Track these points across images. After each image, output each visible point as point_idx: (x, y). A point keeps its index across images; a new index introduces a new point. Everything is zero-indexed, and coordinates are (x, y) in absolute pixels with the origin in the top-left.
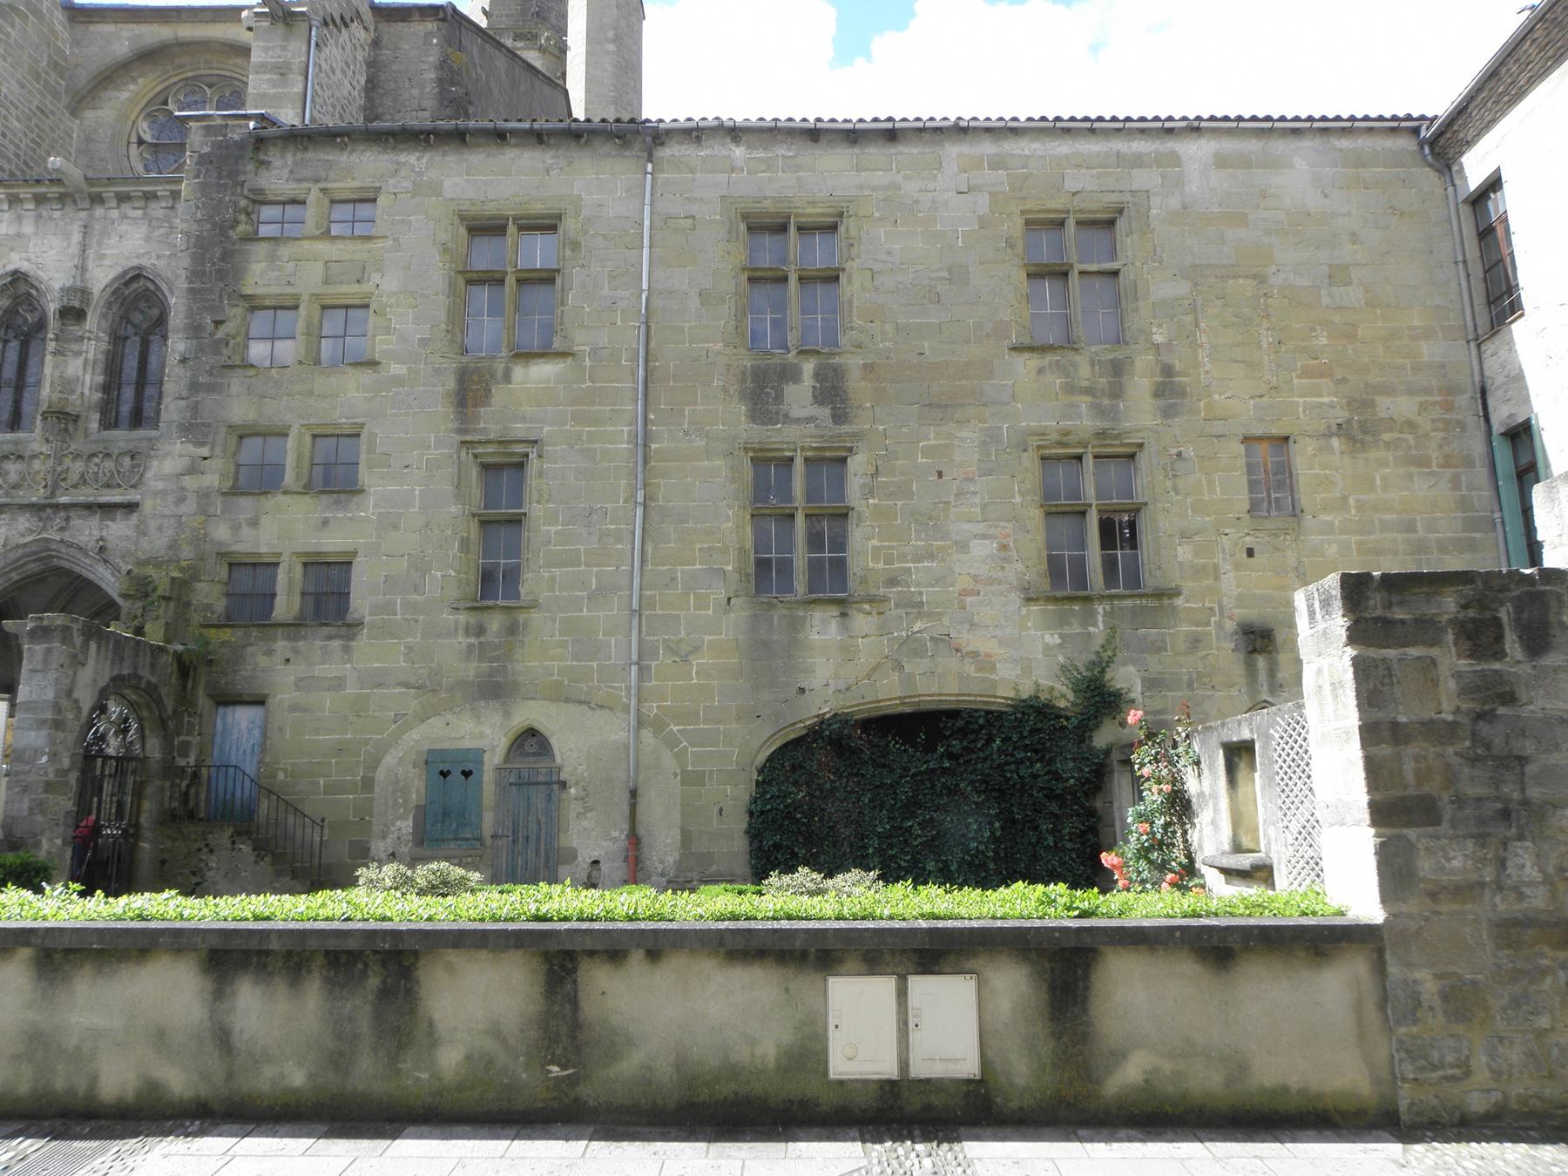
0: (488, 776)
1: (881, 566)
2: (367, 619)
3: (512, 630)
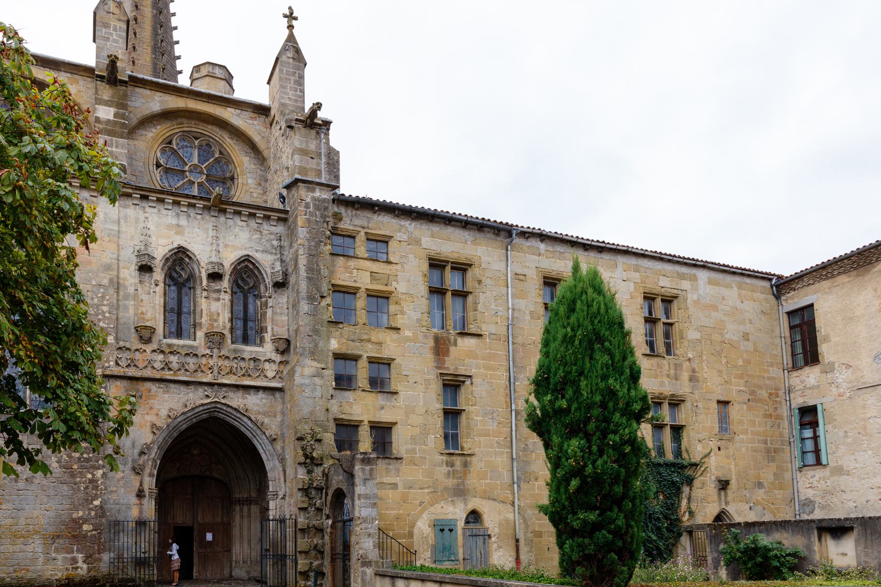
0: (460, 532)
3: (466, 465)
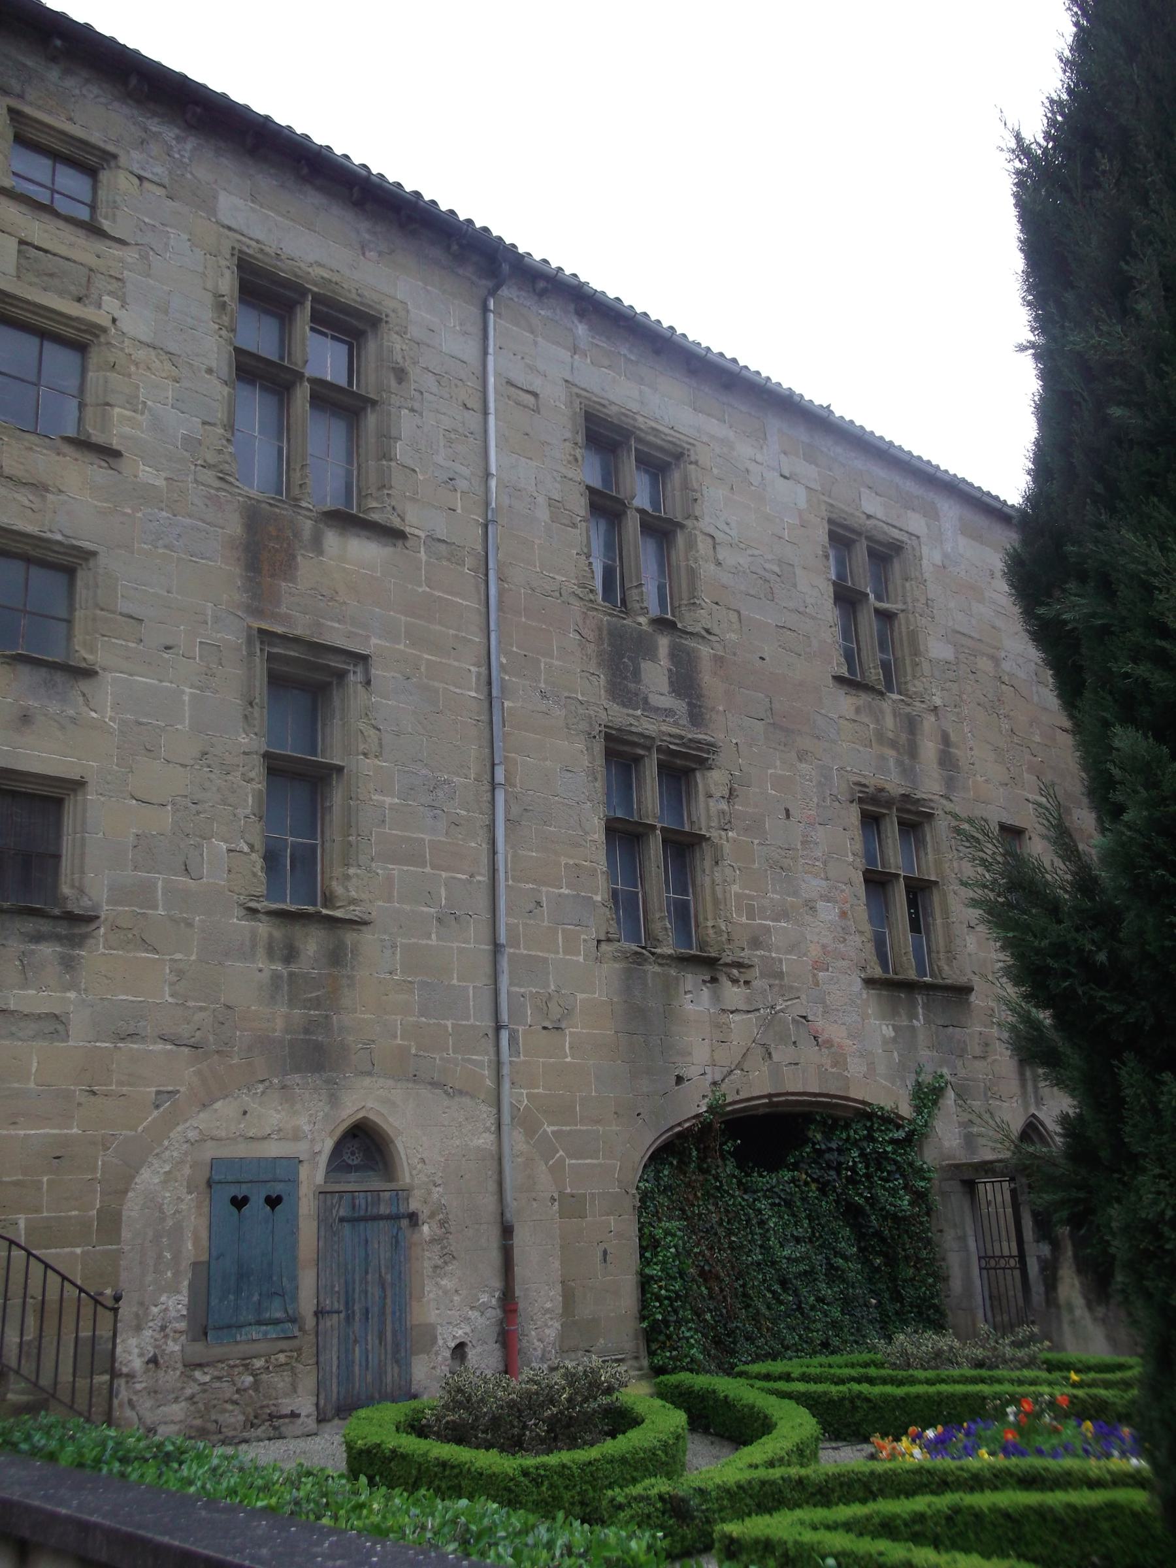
0: (306, 1206)
1: (744, 920)
2: (105, 911)
3: (336, 957)
